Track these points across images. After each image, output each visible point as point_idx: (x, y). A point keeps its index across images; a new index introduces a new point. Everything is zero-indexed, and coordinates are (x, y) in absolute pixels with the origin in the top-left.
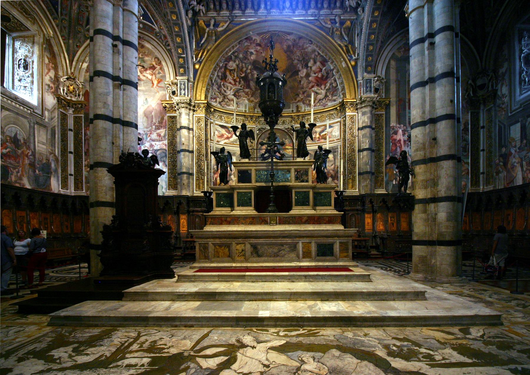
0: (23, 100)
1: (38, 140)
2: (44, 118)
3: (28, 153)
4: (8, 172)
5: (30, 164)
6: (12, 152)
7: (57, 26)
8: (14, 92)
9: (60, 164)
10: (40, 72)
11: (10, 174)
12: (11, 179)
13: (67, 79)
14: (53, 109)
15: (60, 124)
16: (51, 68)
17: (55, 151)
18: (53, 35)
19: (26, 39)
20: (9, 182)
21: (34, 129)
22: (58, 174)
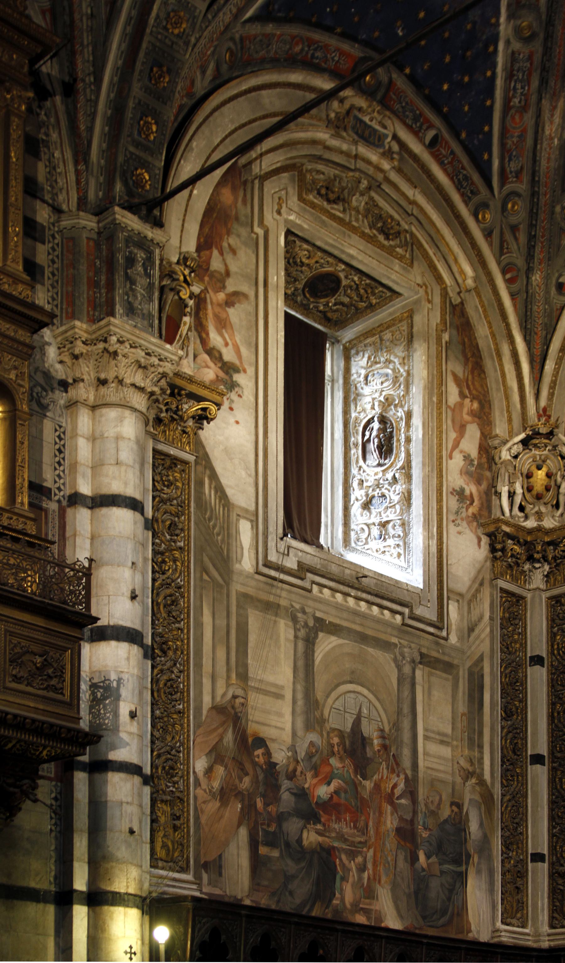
0: (379, 578)
1: (426, 730)
2: (444, 634)
3: (395, 786)
4: (334, 873)
5: (398, 830)
6: (346, 792)
7: (488, 234)
8: (351, 557)
9: (497, 814)
10: (430, 449)
11: (338, 878)
12: (343, 900)
13: (525, 443)
14: (476, 585)
15: (498, 646)
16: (467, 418)
17: (481, 759)
18: (476, 279)
19: (387, 336)
20: (336, 911)
21: (413, 685)
22: (490, 858)
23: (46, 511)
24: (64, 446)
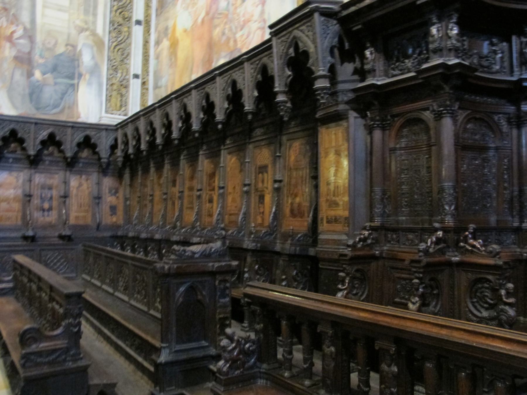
22: (100, 76)
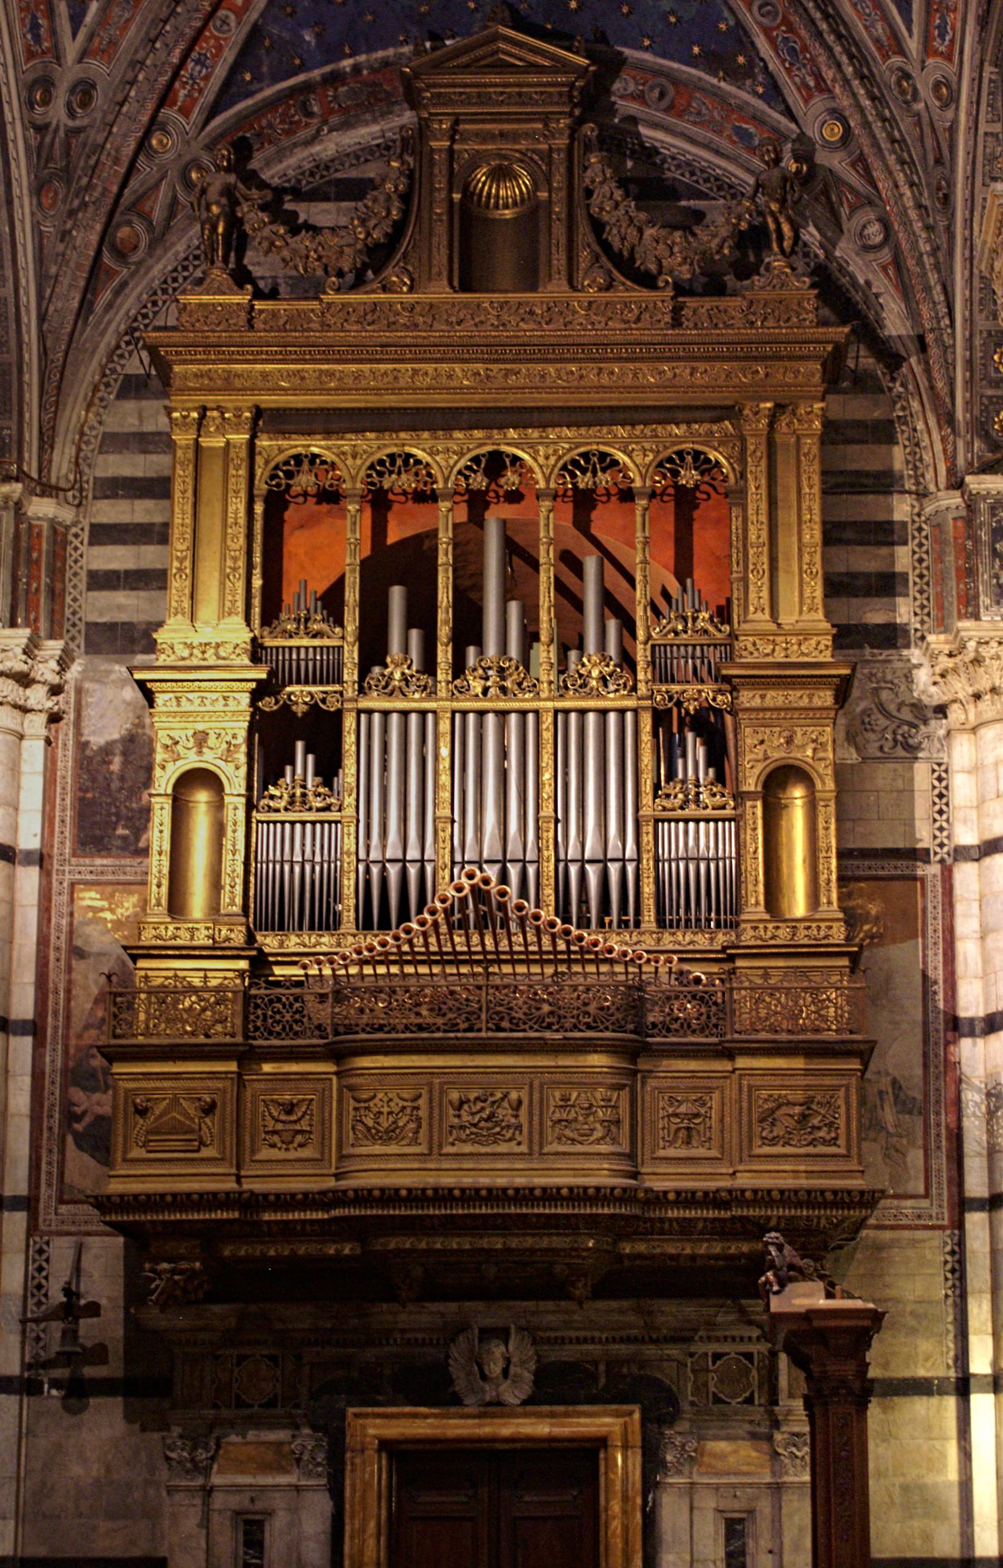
23: (923, 880)
24: (946, 788)
